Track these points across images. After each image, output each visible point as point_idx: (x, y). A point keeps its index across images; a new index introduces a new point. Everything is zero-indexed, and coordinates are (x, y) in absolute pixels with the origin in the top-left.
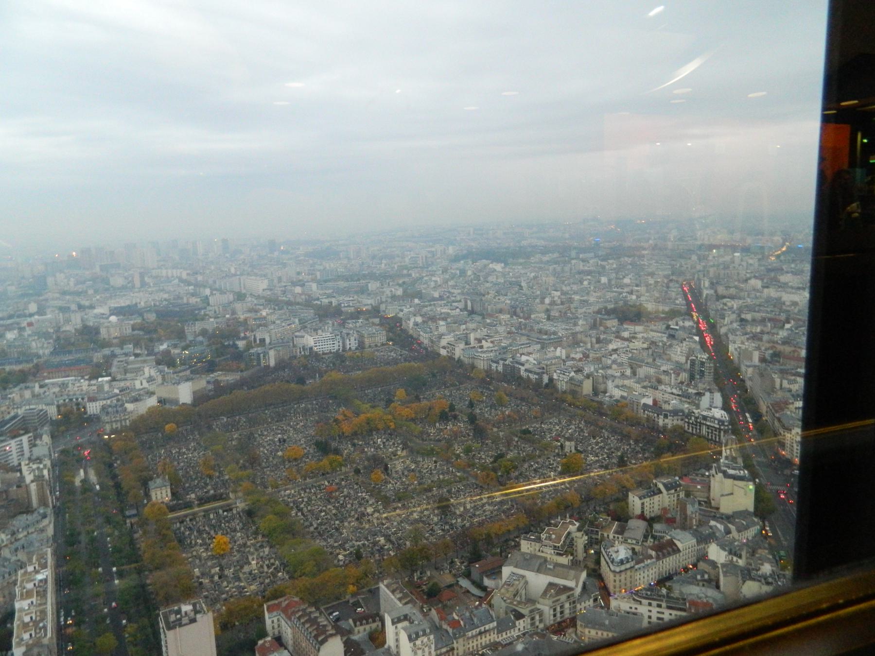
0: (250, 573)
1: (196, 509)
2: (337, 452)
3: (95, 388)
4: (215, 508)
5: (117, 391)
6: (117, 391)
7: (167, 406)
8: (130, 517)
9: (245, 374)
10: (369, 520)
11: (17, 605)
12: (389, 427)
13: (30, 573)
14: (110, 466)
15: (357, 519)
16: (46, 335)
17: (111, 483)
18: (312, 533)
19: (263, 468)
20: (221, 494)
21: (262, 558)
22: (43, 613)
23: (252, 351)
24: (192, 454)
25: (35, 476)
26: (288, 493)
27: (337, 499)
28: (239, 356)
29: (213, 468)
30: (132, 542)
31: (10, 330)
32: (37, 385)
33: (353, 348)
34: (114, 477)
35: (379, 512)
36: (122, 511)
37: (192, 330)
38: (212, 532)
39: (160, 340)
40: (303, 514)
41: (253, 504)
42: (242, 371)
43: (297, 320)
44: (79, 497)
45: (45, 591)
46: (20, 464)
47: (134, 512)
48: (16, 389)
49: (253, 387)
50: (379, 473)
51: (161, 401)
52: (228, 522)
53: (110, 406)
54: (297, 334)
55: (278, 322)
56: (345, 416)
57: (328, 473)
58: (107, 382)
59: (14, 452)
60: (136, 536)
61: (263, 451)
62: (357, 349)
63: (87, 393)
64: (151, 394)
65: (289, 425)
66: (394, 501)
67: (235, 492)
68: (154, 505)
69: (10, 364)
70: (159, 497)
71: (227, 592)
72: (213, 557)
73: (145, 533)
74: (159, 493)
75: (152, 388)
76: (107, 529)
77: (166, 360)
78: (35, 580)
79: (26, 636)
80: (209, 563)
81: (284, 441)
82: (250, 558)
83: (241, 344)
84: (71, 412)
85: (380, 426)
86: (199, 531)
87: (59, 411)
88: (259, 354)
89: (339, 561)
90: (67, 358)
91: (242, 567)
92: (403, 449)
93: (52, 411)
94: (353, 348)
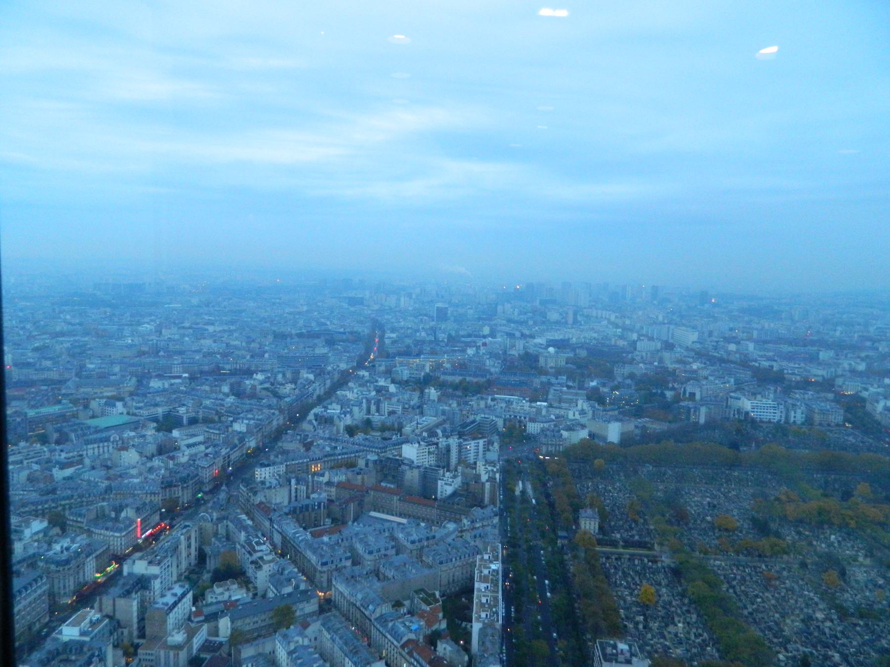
0: (676, 635)
1: (621, 550)
2: (778, 535)
3: (534, 410)
4: (641, 555)
5: (553, 417)
6: (553, 417)
7: (596, 440)
8: (561, 537)
9: (674, 426)
10: (818, 627)
12: (847, 525)
13: (486, 561)
14: (545, 485)
15: (803, 621)
17: (545, 501)
18: (746, 617)
19: (690, 529)
20: (646, 543)
21: (688, 623)
22: (496, 599)
23: (682, 404)
24: (617, 493)
26: (717, 563)
27: (776, 588)
28: (667, 407)
29: (638, 513)
30: (562, 563)
31: (470, 347)
32: (490, 398)
33: (799, 422)
34: (548, 496)
35: (832, 621)
36: (554, 531)
37: (621, 372)
38: (637, 579)
39: (591, 377)
40: (735, 592)
41: (681, 563)
42: (670, 422)
43: (732, 380)
44: (518, 506)
45: (497, 581)
46: (475, 463)
47: (564, 534)
48: (475, 398)
49: (681, 442)
50: (833, 575)
51: (592, 435)
52: (653, 573)
53: (548, 430)
54: (732, 394)
55: (710, 378)
56: (788, 497)
57: (766, 556)
58: (545, 407)
59: (472, 452)
60: (566, 557)
61: (692, 510)
62: (803, 424)
63: (529, 413)
64: (583, 426)
65: (719, 490)
66: (852, 615)
67: (661, 544)
68: (585, 533)
69: (470, 375)
70: (587, 527)
71: (652, 646)
72: (637, 604)
73: (575, 557)
74: (588, 522)
75: (583, 421)
76: (540, 543)
77: (595, 397)
78: (490, 568)
79: (483, 615)
80: (634, 609)
81: (714, 506)
82: (676, 619)
83: (669, 394)
84: (514, 427)
85: (836, 521)
86: (624, 572)
87: (505, 424)
88: (689, 409)
89: (779, 660)
90: (513, 379)
91: (667, 625)
92: (866, 556)
93: (500, 423)
94: (799, 422)
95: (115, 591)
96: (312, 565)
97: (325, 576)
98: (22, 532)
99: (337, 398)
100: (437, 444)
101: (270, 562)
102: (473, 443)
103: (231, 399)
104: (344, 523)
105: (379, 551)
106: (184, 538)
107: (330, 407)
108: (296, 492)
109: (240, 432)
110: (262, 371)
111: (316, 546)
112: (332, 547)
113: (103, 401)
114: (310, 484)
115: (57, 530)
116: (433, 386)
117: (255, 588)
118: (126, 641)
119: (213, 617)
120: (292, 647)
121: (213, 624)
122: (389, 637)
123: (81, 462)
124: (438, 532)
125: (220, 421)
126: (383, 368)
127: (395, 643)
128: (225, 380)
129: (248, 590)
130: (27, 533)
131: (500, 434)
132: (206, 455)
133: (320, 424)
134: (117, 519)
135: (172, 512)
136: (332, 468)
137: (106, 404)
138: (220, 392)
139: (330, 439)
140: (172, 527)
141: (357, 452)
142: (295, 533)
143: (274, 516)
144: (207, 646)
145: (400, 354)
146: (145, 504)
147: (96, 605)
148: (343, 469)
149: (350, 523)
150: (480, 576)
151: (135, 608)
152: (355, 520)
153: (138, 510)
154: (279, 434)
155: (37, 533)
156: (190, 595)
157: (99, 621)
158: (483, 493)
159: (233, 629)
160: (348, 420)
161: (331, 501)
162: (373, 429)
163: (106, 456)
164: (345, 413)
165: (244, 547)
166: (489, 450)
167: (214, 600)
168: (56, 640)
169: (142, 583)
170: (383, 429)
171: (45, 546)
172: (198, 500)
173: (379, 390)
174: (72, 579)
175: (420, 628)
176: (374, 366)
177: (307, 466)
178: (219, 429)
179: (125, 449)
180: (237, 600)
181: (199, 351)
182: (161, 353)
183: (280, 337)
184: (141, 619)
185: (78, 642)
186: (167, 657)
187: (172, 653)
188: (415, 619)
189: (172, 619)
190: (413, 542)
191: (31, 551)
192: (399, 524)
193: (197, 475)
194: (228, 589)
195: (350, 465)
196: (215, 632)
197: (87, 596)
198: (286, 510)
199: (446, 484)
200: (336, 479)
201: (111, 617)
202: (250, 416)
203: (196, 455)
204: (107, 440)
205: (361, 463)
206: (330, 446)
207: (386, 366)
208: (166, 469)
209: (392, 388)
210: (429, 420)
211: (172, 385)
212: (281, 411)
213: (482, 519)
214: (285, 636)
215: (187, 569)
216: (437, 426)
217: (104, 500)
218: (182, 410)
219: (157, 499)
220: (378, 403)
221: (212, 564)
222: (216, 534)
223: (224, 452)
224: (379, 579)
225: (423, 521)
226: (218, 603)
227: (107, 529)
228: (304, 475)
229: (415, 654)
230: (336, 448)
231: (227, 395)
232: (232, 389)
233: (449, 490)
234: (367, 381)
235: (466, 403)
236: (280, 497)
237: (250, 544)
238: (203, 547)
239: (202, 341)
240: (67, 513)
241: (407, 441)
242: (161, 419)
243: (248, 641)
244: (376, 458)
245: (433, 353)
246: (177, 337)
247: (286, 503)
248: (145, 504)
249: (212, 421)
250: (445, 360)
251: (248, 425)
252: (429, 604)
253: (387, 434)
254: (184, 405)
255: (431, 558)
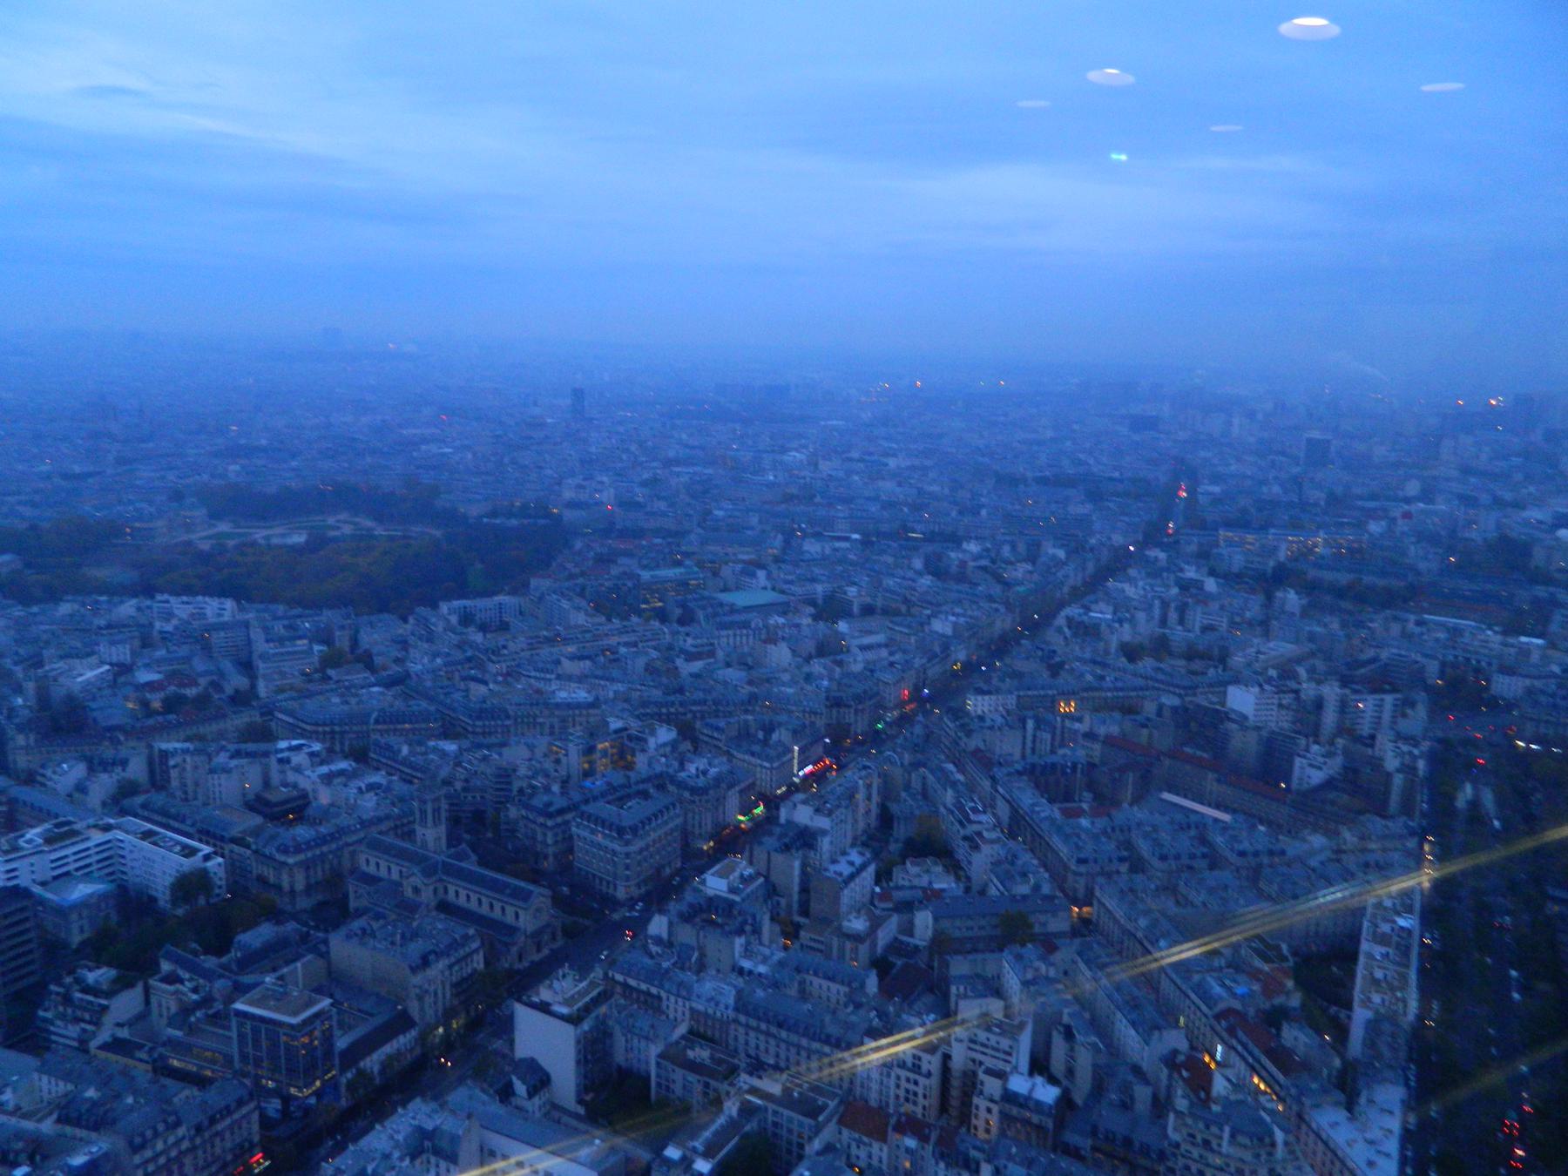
3: (1512, 650)
6: (1556, 669)
11: (1365, 946)
16: (1432, 539)
22: (1404, 978)
25: (1403, 764)
46: (1373, 737)
53: (1543, 692)
93: (1433, 667)
95: (770, 842)
96: (1061, 860)
97: (1082, 881)
98: (646, 741)
99: (1107, 594)
100: (1297, 692)
101: (992, 842)
102: (1372, 699)
103: (926, 581)
104: (1116, 804)
105: (1177, 857)
106: (861, 780)
107: (1093, 607)
108: (1034, 742)
109: (943, 635)
110: (977, 538)
111: (1068, 830)
112: (1095, 837)
113: (739, 567)
114: (1058, 732)
115: (686, 746)
116: (1292, 586)
117: (969, 879)
118: (783, 914)
119: (906, 907)
120: (1029, 976)
121: (906, 917)
122: (1193, 996)
123: (712, 654)
124: (1293, 847)
125: (909, 613)
126: (1192, 548)
127: (1204, 1008)
128: (916, 549)
129: (958, 878)
130: (652, 743)
131: (1430, 689)
132: (892, 664)
133: (1075, 635)
134: (765, 742)
135: (840, 745)
136: (1096, 710)
137: (743, 572)
138: (909, 567)
139: (1095, 662)
140: (841, 768)
141: (1141, 689)
142: (1034, 805)
143: (1000, 773)
144: (896, 947)
145: (1229, 525)
146: (804, 726)
147: (747, 854)
148: (1117, 715)
149: (1125, 805)
150: (1375, 933)
151: (797, 872)
152: (1137, 800)
153: (795, 732)
154: (1002, 646)
155: (664, 745)
156: (872, 869)
157: (751, 879)
158: (1387, 793)
159: (935, 930)
160: (1126, 633)
161: (1092, 766)
162: (1171, 654)
163: (746, 649)
164: (1121, 622)
165: (952, 812)
166: (1404, 715)
167: (907, 883)
168: (696, 890)
169: (805, 839)
170: (1191, 654)
171: (676, 764)
172: (877, 732)
173: (1185, 586)
174: (709, 815)
175: (1251, 994)
176: (1177, 542)
177: (1053, 702)
178: (909, 627)
179: (772, 639)
180: (943, 890)
181: (876, 499)
182: (818, 499)
183: (1009, 482)
184: (805, 890)
185: (726, 900)
186: (842, 949)
187: (848, 945)
188: (1242, 978)
189: (848, 896)
190: (1242, 854)
191: (658, 769)
192: (1216, 820)
193: (878, 694)
194: (928, 871)
195: (1129, 710)
196: (909, 929)
197: (730, 842)
198: (1018, 767)
199: (1311, 765)
200: (1102, 731)
201: (767, 878)
202: (958, 610)
203: (874, 662)
204: (745, 625)
205: (1150, 708)
206: (1093, 674)
207: (1200, 545)
208: (831, 679)
209: (1211, 585)
210: (1280, 648)
211: (836, 550)
212: (1009, 606)
213: (1385, 837)
214: (1019, 957)
215: (865, 832)
216: (1299, 661)
217: (746, 712)
218: (852, 591)
219: (820, 723)
220: (1182, 610)
221: (901, 831)
222: (907, 787)
223: (918, 662)
224: (1178, 902)
225: (1261, 822)
226: (912, 888)
227: (753, 754)
228: (1049, 717)
229: (1240, 1034)
230: (1102, 678)
231: (919, 573)
232: (927, 564)
233: (1317, 777)
234: (1163, 569)
235: (1360, 624)
236: (1009, 746)
237: (961, 808)
238: (889, 804)
239: (880, 483)
240: (698, 724)
241: (1236, 681)
242: (820, 602)
243: (958, 952)
244: (1176, 701)
245: (1295, 525)
246: (841, 474)
247: (1017, 756)
248: (804, 726)
249: (897, 613)
250: (1320, 543)
251: (955, 624)
252: (1267, 959)
253: (1197, 665)
254: (854, 584)
255: (1275, 887)
